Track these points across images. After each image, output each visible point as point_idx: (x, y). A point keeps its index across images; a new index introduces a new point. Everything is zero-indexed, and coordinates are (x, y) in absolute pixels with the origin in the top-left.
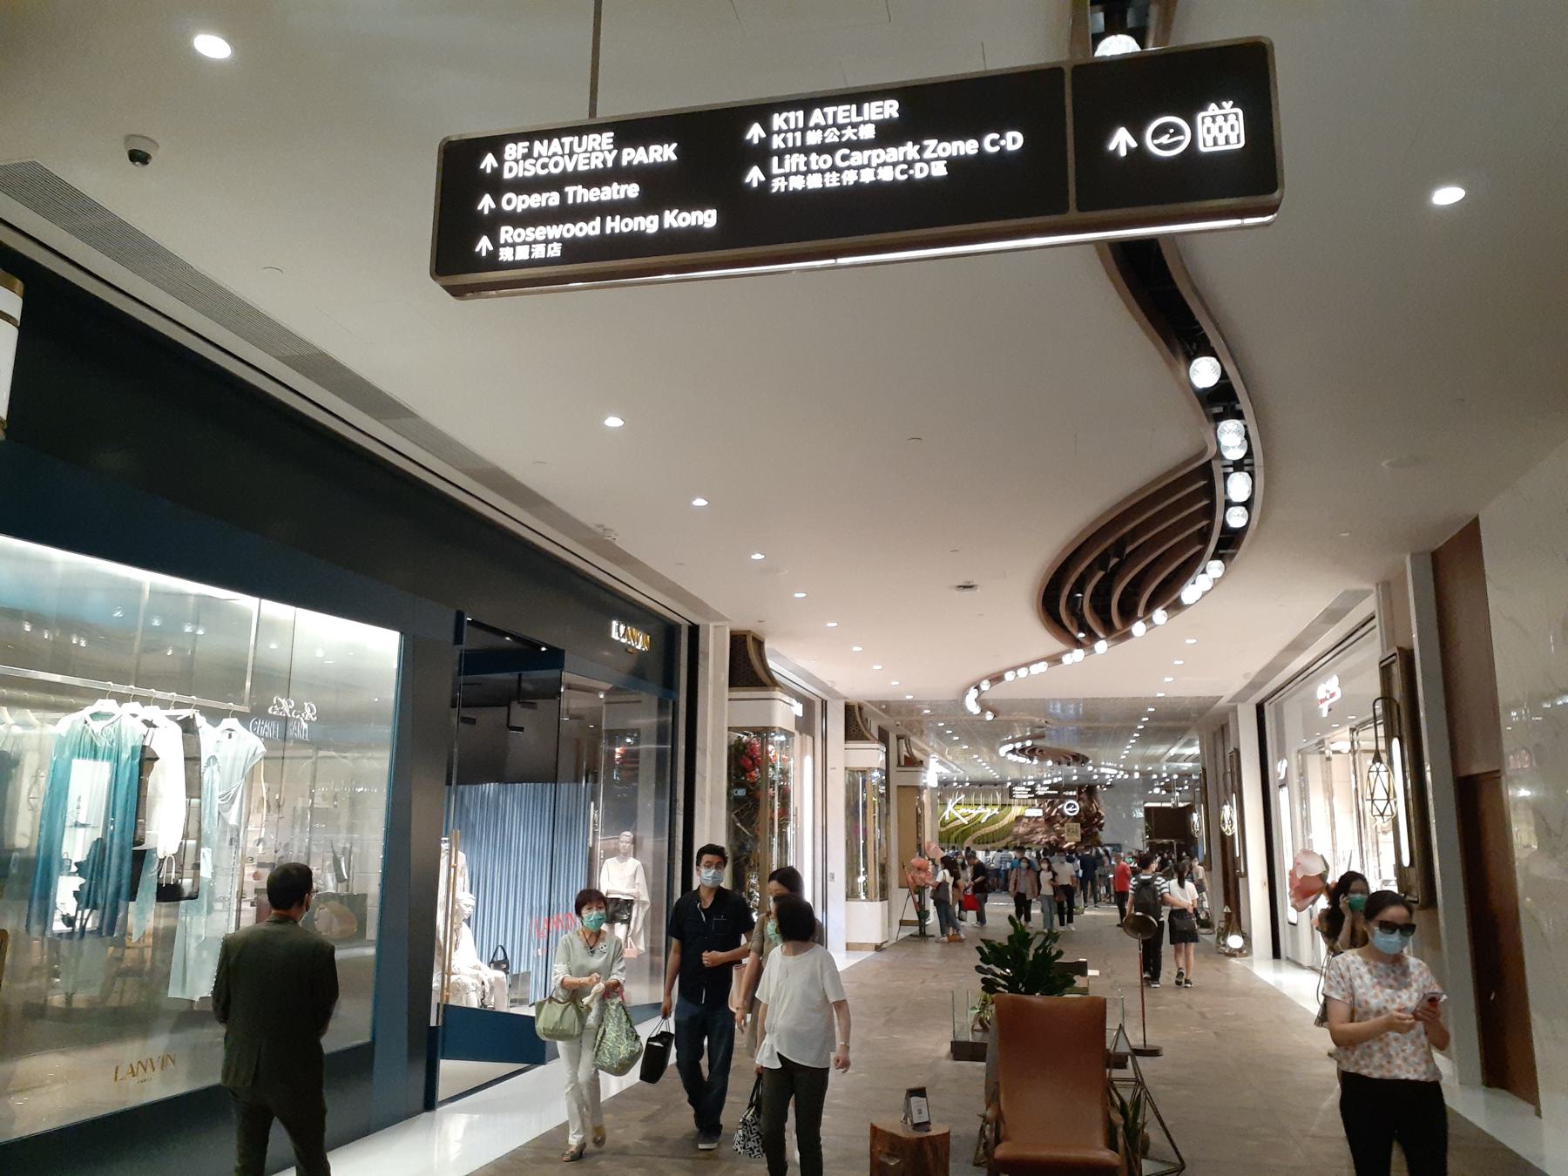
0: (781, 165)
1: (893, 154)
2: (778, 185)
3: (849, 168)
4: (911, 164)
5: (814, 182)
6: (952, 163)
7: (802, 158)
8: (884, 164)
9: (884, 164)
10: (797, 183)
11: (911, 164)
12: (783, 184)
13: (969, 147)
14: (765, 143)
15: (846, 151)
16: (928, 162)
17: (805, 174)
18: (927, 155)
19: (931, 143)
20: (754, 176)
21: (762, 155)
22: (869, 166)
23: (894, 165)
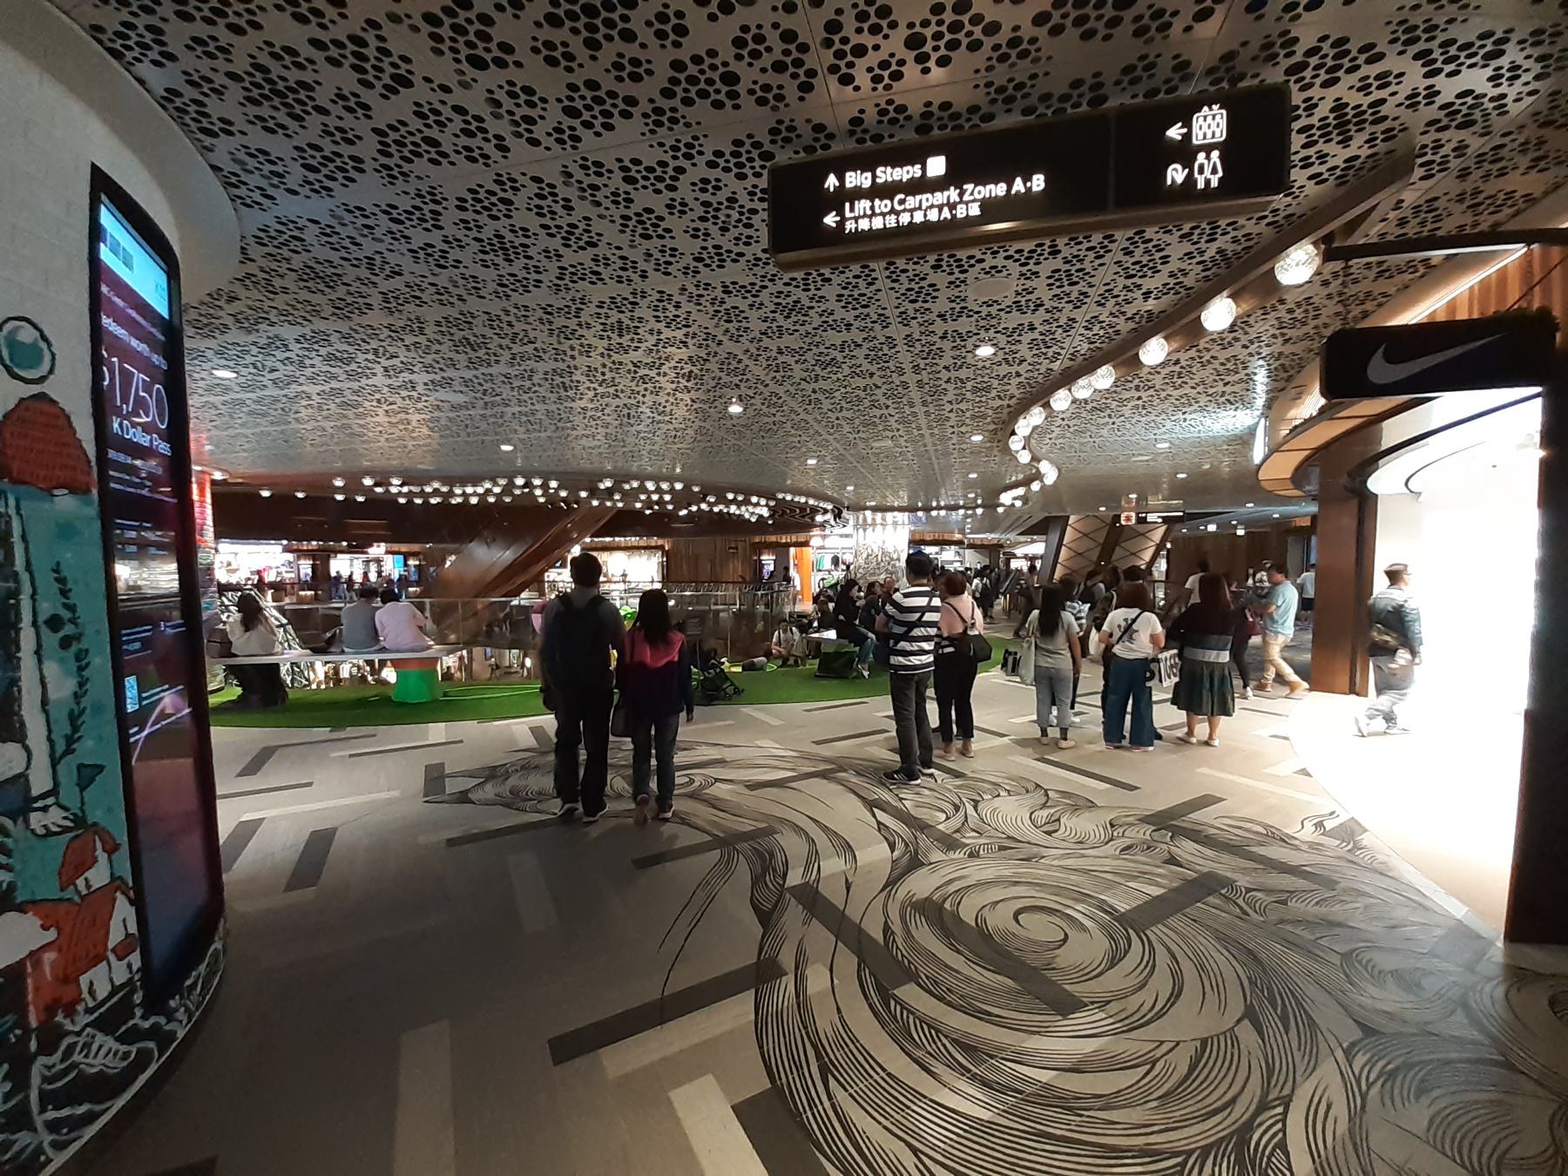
0: (852, 210)
3: (905, 210)
4: (952, 207)
5: (878, 223)
6: (985, 204)
7: (868, 204)
8: (932, 206)
9: (932, 206)
10: (864, 225)
13: (1000, 190)
15: (902, 196)
16: (967, 203)
17: (870, 217)
18: (966, 197)
19: (969, 187)
22: (920, 208)
23: (940, 208)
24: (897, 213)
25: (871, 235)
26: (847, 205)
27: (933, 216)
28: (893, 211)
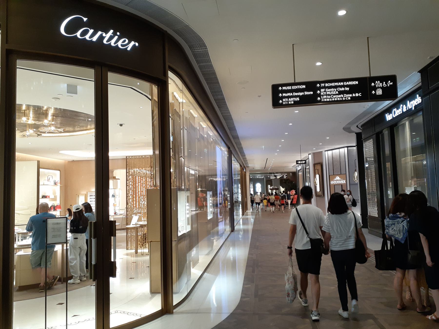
1: (340, 96)
2: (323, 100)
4: (342, 98)
5: (328, 100)
10: (325, 100)
13: (351, 95)
14: (320, 93)
21: (320, 95)
23: (340, 98)
27: (339, 99)
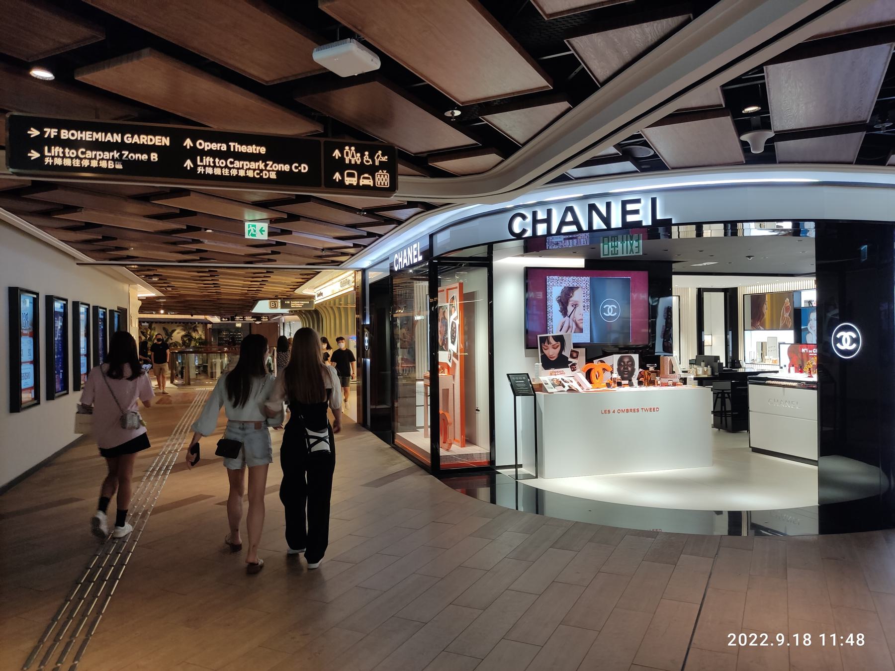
0: (201, 161)
2: (200, 170)
4: (262, 171)
5: (218, 172)
7: (212, 160)
8: (249, 169)
9: (249, 169)
10: (209, 171)
11: (262, 171)
12: (203, 170)
13: (286, 168)
16: (269, 171)
18: (268, 168)
19: (270, 163)
20: (188, 164)
22: (242, 168)
23: (254, 170)
24: (230, 169)
25: (213, 177)
26: (199, 158)
27: (250, 174)
28: (226, 167)
